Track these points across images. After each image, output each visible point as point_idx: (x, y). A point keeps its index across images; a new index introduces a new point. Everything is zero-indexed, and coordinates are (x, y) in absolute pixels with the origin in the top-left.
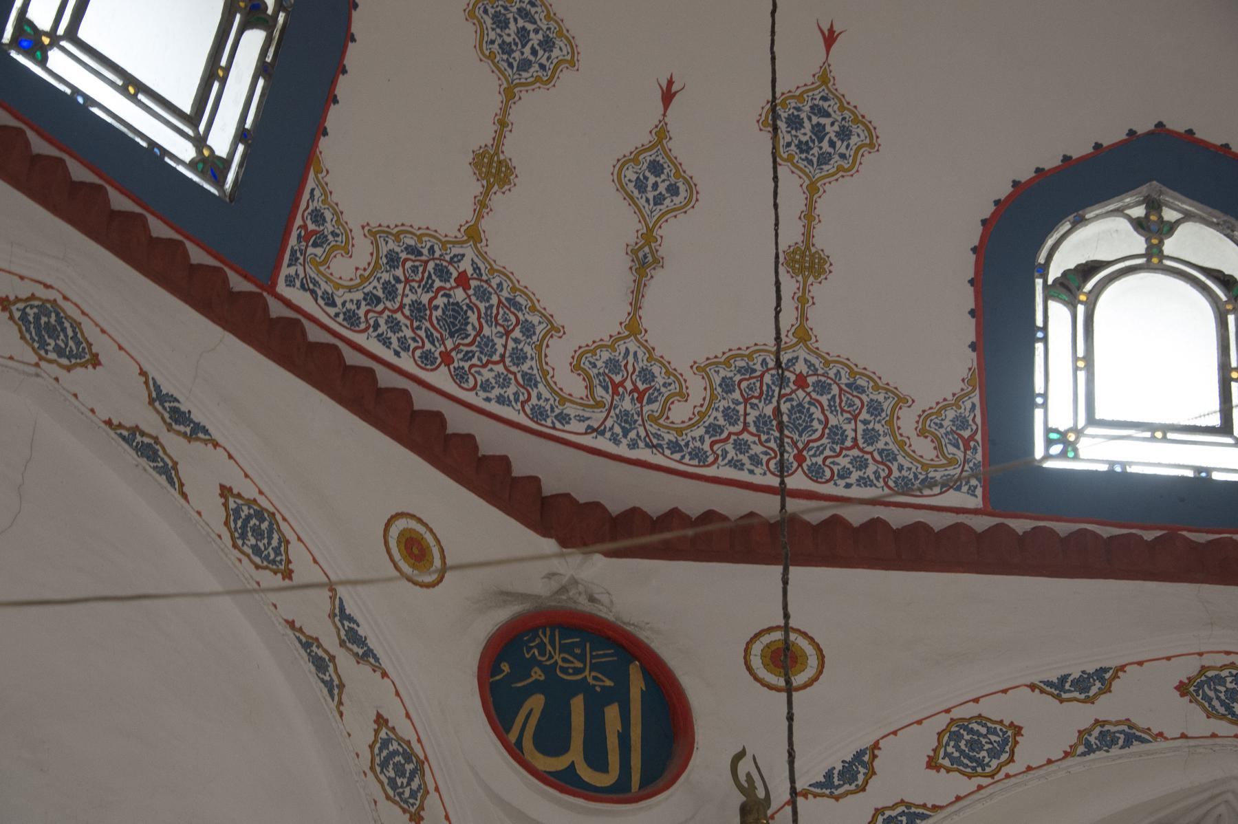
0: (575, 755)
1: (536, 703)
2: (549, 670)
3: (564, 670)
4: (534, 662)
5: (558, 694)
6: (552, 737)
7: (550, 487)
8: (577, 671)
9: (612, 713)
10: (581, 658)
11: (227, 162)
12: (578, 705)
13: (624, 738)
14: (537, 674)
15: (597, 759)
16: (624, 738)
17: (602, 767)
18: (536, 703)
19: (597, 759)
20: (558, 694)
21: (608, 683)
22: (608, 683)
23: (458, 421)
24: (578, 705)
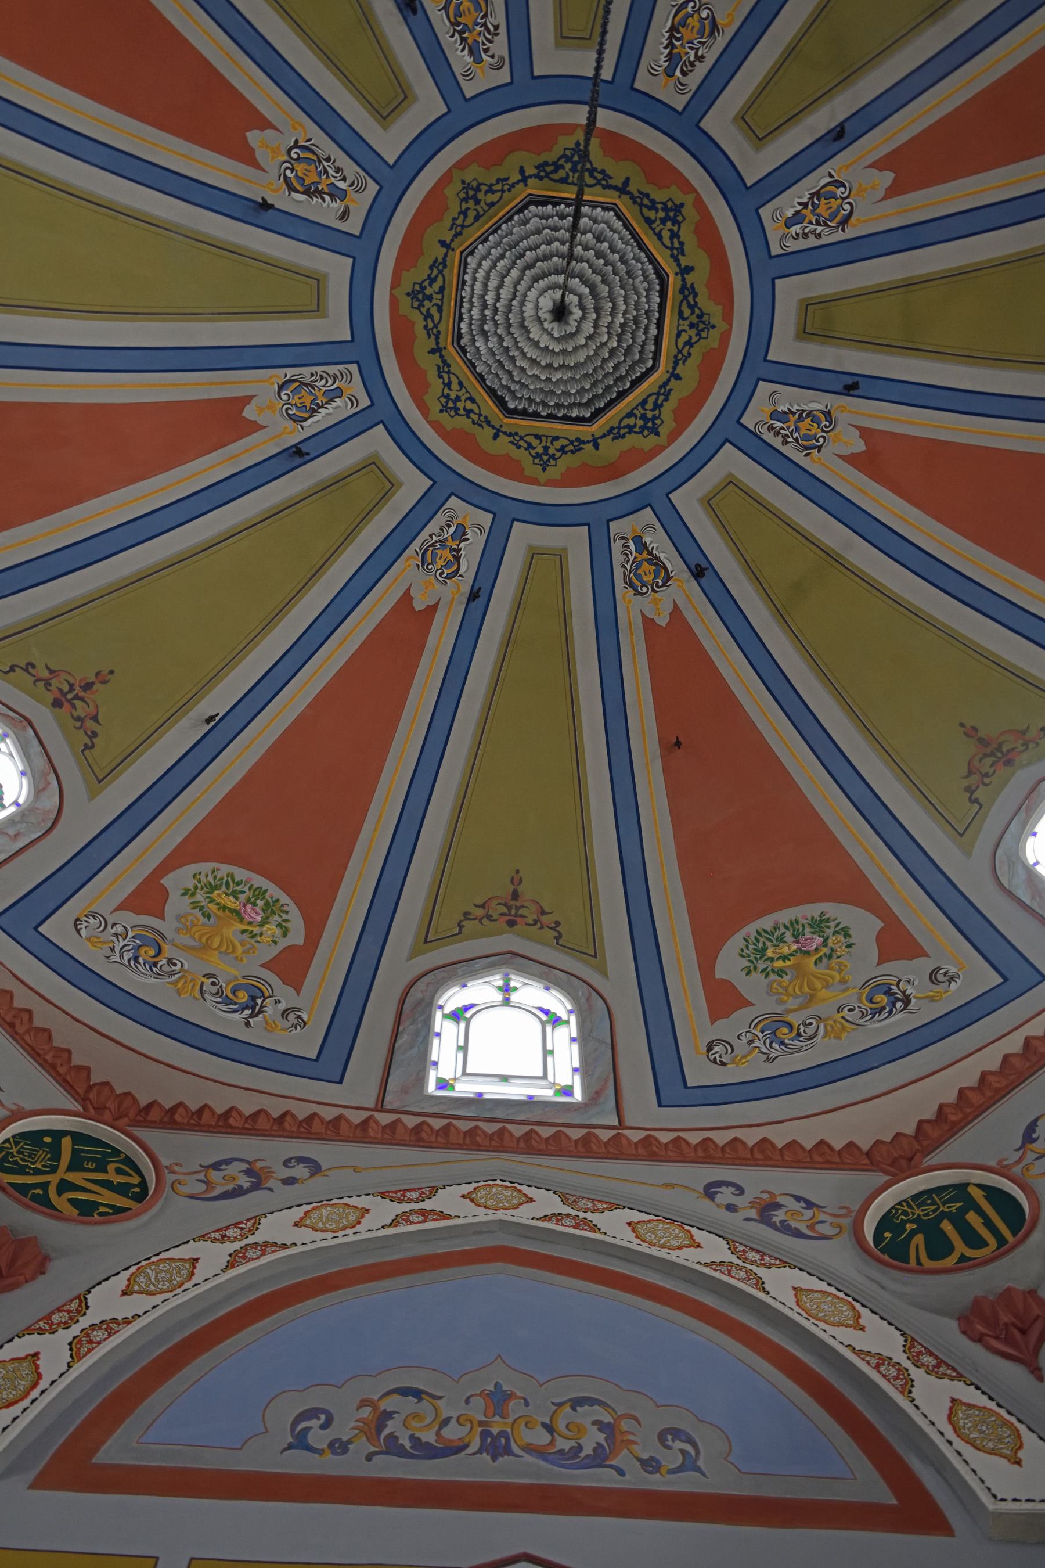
1: (919, 1239)
2: (917, 1220)
3: (927, 1215)
4: (904, 1222)
6: (939, 1248)
7: (865, 1144)
8: (934, 1211)
9: (972, 1217)
10: (934, 1203)
11: (572, 1087)
12: (947, 1226)
13: (989, 1224)
14: (909, 1227)
15: (974, 1240)
16: (989, 1224)
17: (985, 1244)
19: (974, 1240)
21: (958, 1205)
22: (958, 1205)
23: (780, 1137)
24: (947, 1226)
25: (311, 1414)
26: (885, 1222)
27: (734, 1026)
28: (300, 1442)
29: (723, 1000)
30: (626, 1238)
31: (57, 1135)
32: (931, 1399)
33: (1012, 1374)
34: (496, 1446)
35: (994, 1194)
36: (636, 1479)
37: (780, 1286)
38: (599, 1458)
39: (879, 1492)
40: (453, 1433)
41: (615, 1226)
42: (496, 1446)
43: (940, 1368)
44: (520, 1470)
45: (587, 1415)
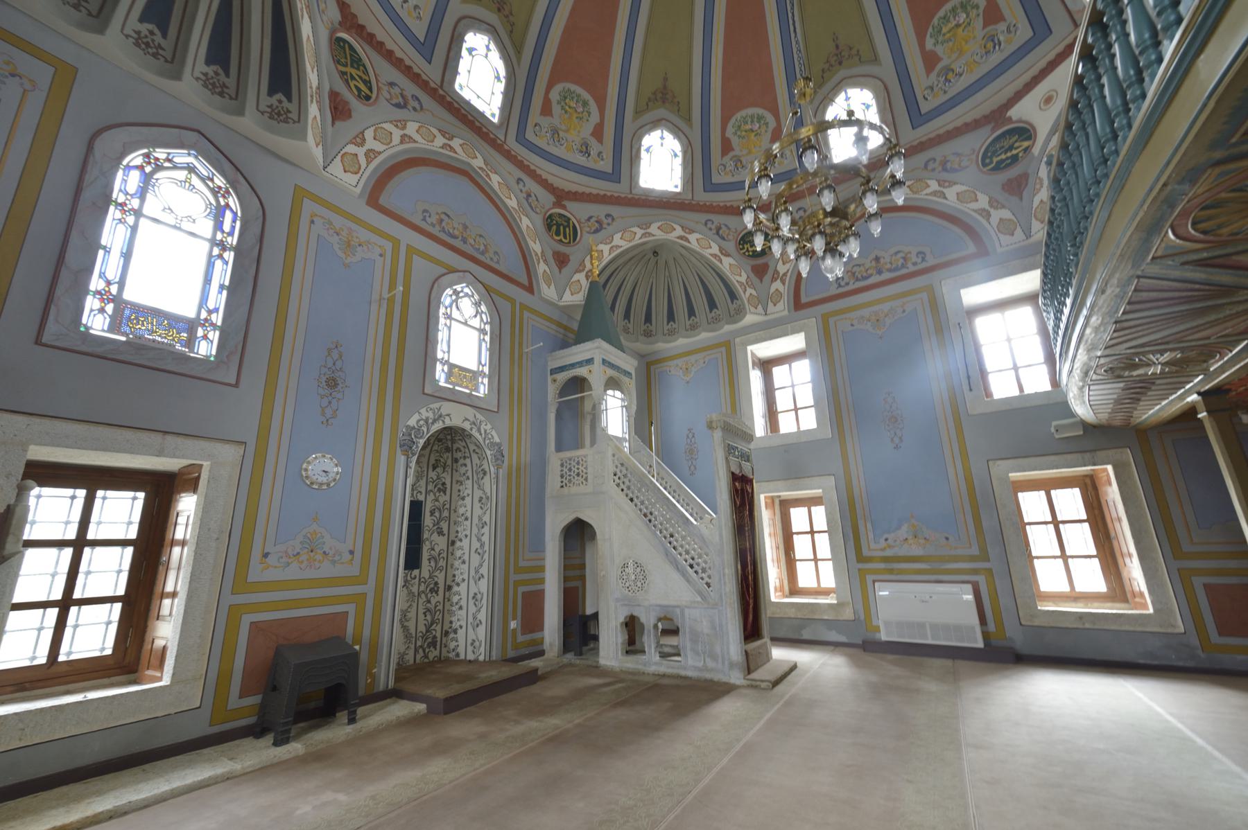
0: (562, 237)
1: (554, 228)
5: (558, 226)
6: (558, 233)
18: (554, 228)
20: (558, 226)
23: (539, 172)
25: (425, 211)
26: (550, 216)
27: (545, 122)
28: (424, 219)
29: (546, 110)
30: (496, 187)
31: (345, 41)
32: (542, 268)
33: (556, 269)
34: (464, 241)
35: (574, 227)
36: (488, 261)
37: (525, 222)
38: (483, 253)
39: (526, 283)
40: (456, 232)
41: (495, 180)
42: (464, 241)
43: (545, 261)
44: (467, 249)
45: (482, 241)
